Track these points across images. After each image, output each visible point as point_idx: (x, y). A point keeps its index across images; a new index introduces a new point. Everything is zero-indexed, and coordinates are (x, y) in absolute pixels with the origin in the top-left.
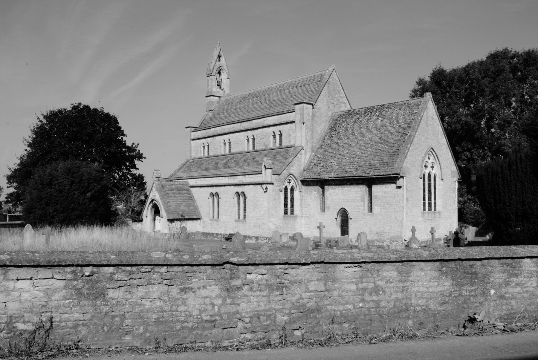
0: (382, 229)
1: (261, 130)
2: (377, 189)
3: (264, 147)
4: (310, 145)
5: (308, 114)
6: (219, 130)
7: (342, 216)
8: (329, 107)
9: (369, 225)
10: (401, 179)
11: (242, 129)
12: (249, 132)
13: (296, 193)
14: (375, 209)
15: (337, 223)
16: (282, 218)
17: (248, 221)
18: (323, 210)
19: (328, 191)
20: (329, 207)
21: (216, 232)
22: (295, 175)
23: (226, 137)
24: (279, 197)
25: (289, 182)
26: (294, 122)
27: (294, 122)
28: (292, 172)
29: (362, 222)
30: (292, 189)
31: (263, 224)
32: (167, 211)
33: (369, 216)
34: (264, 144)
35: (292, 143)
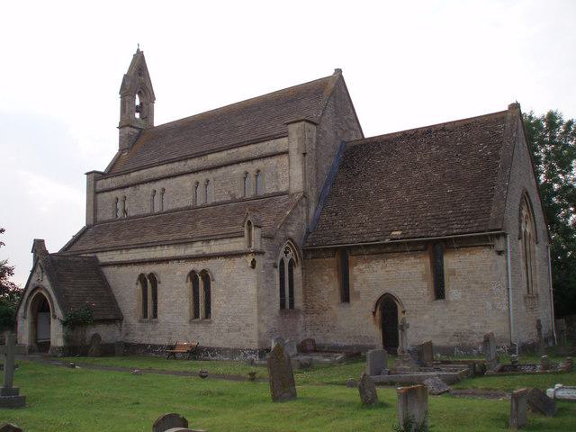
0: (466, 327)
1: (223, 170)
2: (451, 262)
3: (229, 199)
4: (314, 190)
5: (310, 139)
6: (145, 173)
7: (384, 308)
8: (337, 134)
9: (440, 322)
10: (502, 240)
11: (187, 170)
12: (200, 174)
13: (297, 272)
14: (453, 293)
15: (375, 320)
16: (278, 314)
17: (216, 321)
18: (345, 297)
19: (356, 265)
20: (358, 295)
21: (152, 342)
22: (295, 240)
23: (158, 186)
24: (273, 276)
25: (286, 253)
26: (286, 153)
27: (286, 153)
28: (291, 234)
29: (426, 317)
30: (291, 264)
31: (247, 325)
32: (63, 307)
33: (439, 304)
34: (229, 192)
35: (283, 188)
